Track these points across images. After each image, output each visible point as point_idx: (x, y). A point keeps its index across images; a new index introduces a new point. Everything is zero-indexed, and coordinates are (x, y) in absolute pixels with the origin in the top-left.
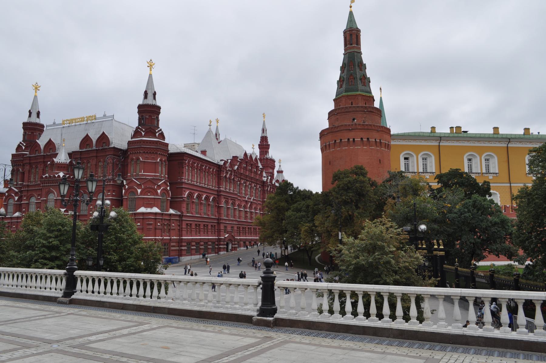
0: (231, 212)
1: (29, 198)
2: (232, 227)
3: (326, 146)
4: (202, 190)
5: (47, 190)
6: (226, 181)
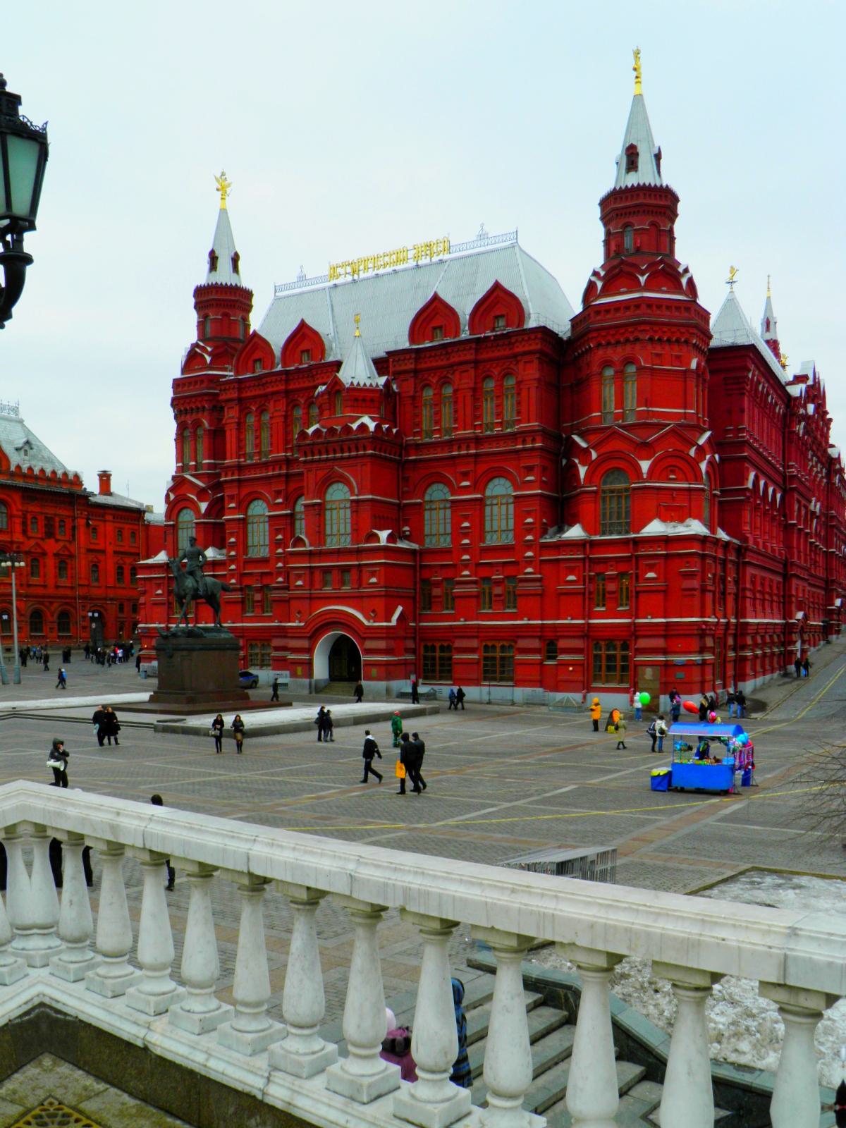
1: (243, 506)
5: (321, 474)
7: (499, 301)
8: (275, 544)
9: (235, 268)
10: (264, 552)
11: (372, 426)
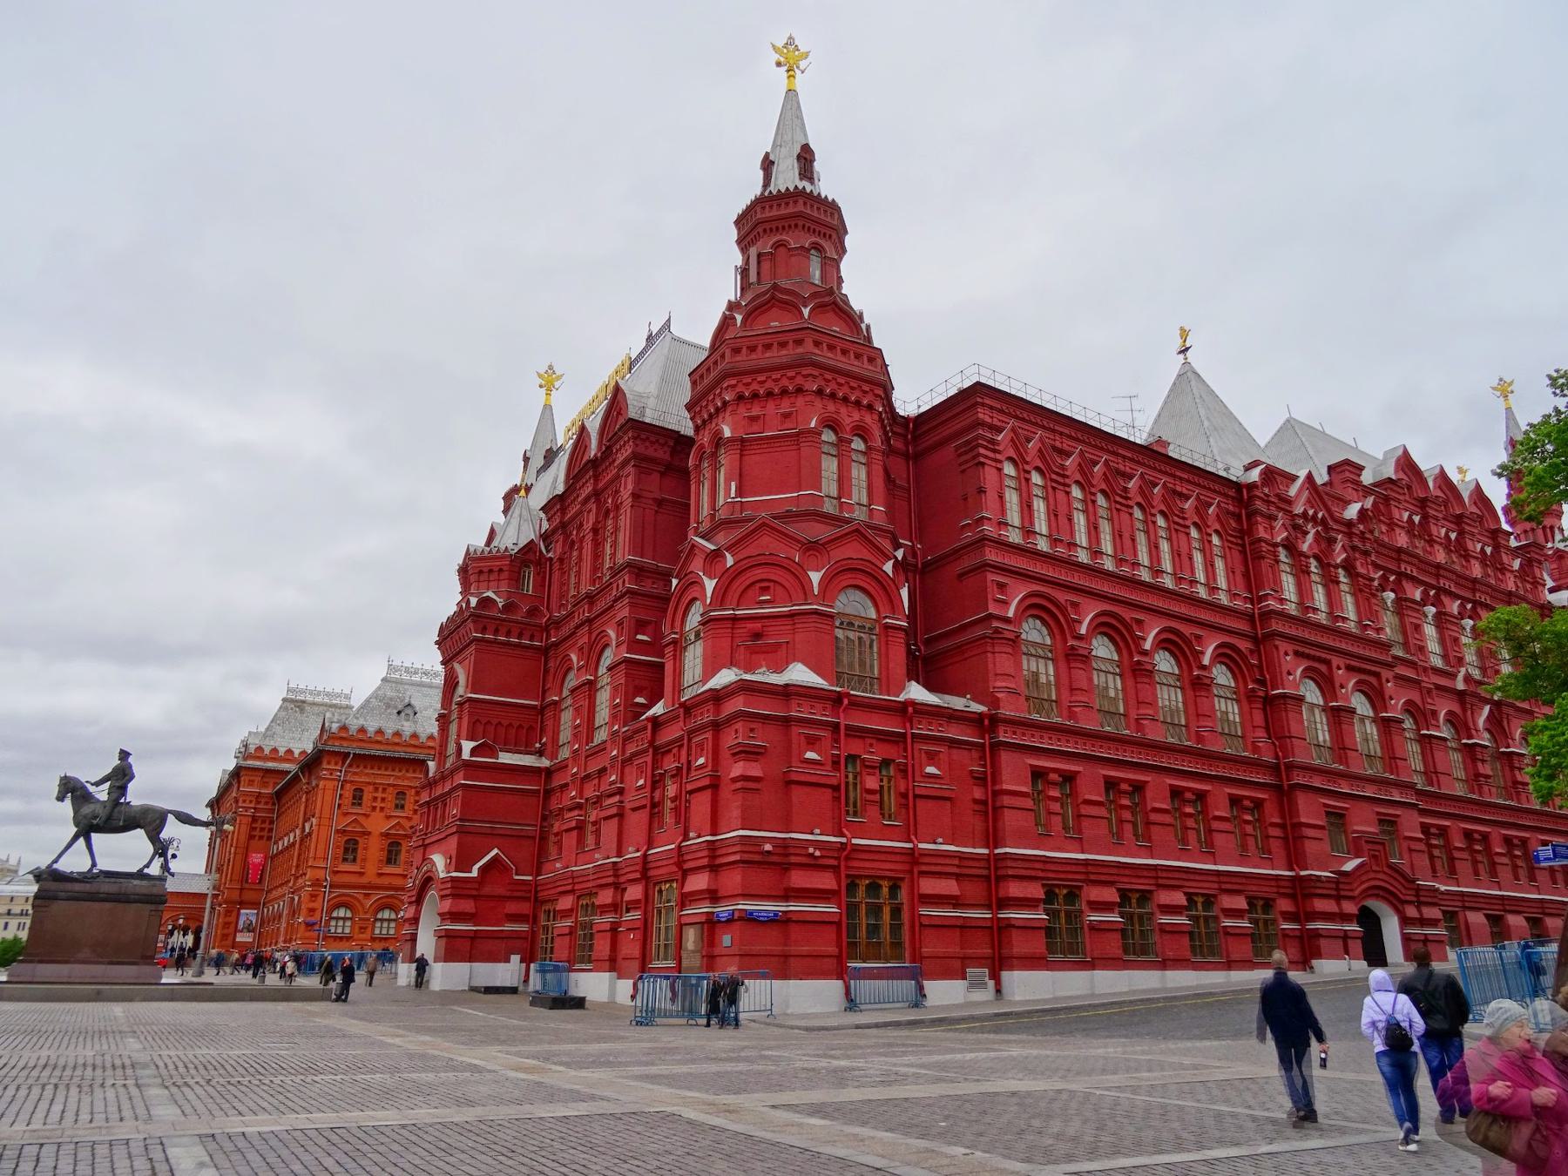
0: (1366, 734)
2: (1388, 823)
6: (1301, 572)
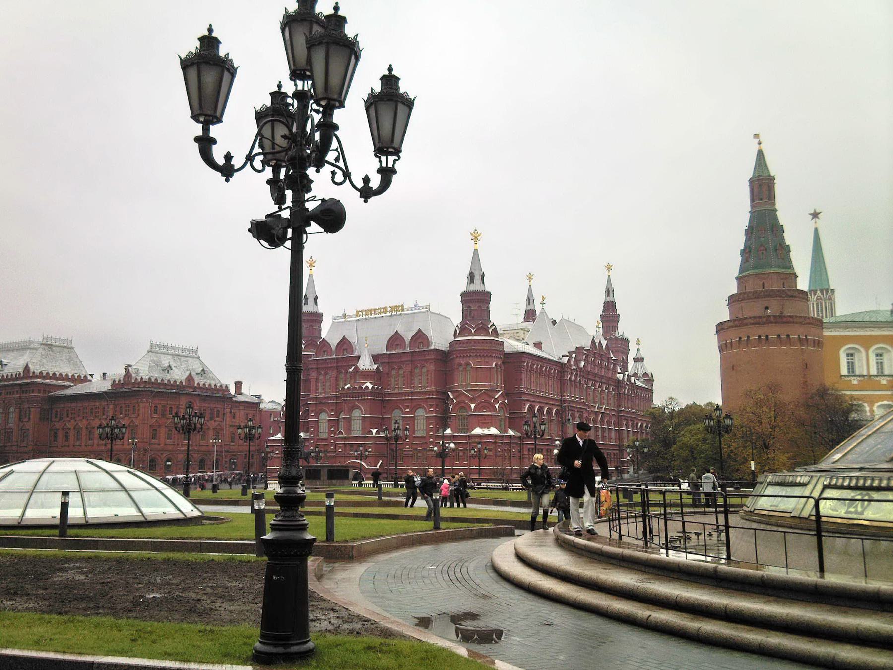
1: (317, 415)
3: (726, 344)
4: (543, 401)
7: (420, 337)
8: (330, 432)
9: (316, 303)
10: (325, 436)
11: (370, 386)
